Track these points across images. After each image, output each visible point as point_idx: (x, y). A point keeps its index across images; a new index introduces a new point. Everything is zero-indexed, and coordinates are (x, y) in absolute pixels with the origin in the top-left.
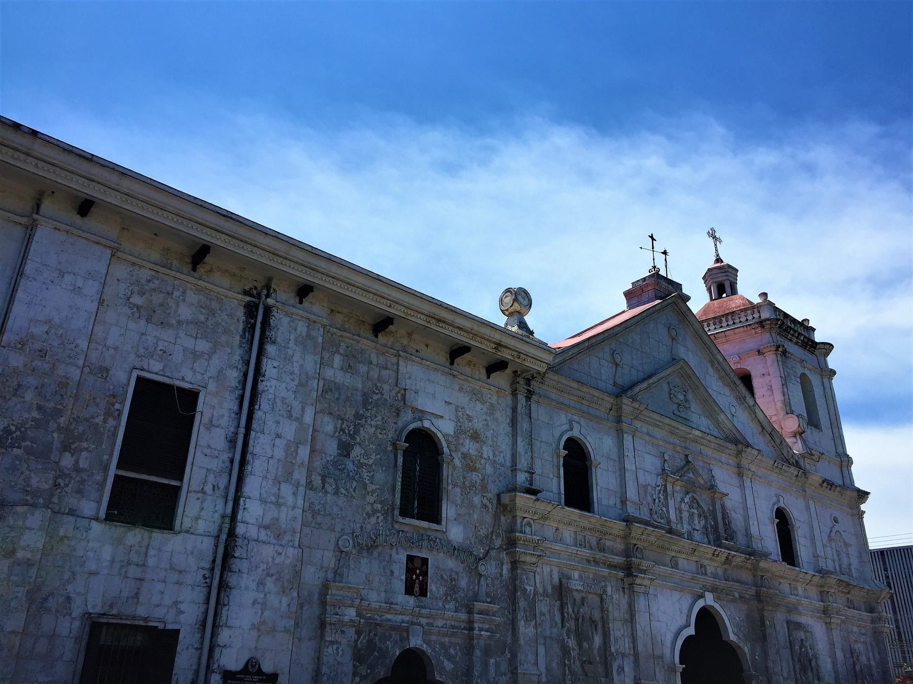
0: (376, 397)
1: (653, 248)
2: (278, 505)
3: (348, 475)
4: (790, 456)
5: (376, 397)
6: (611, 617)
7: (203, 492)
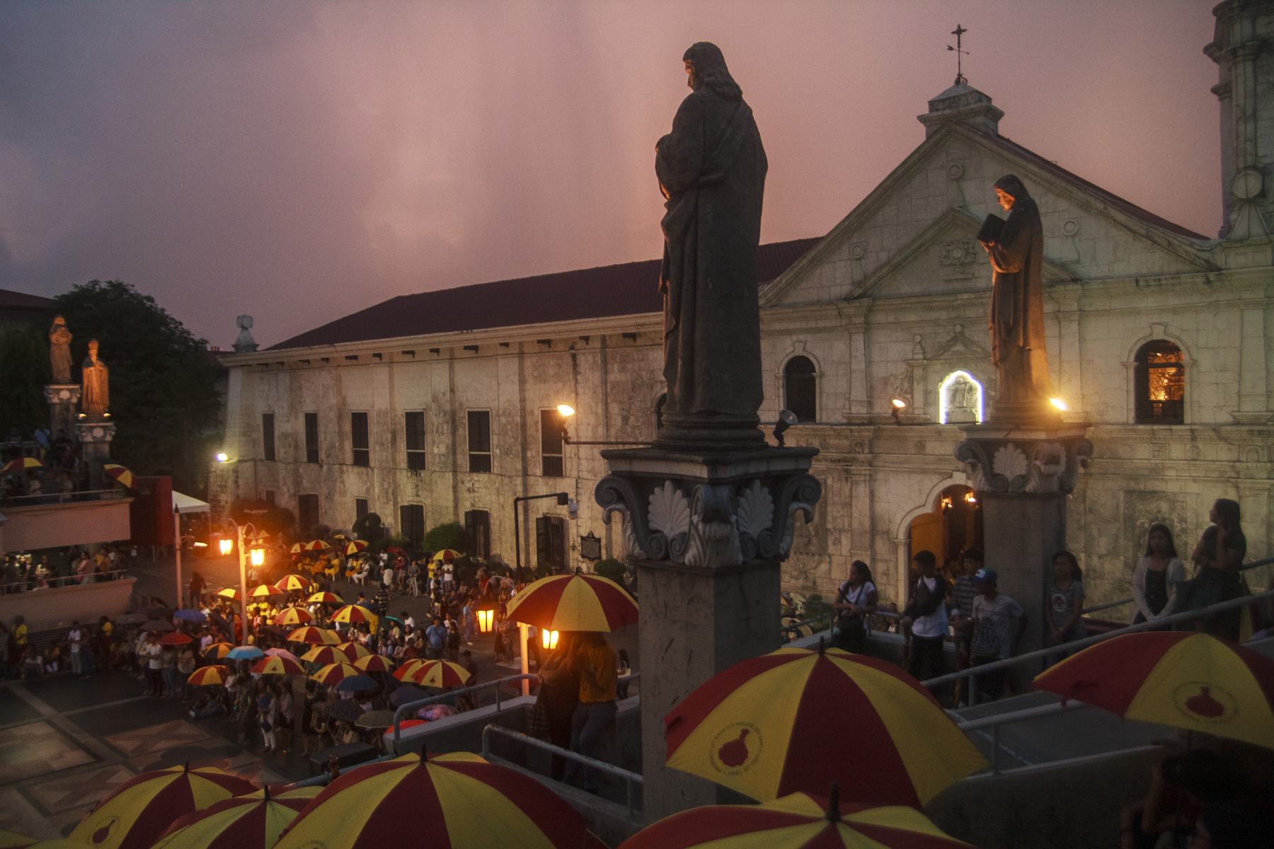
0: (638, 382)
1: (959, 47)
2: (593, 460)
3: (628, 435)
4: (1193, 256)
5: (638, 382)
6: (830, 502)
7: (571, 458)
